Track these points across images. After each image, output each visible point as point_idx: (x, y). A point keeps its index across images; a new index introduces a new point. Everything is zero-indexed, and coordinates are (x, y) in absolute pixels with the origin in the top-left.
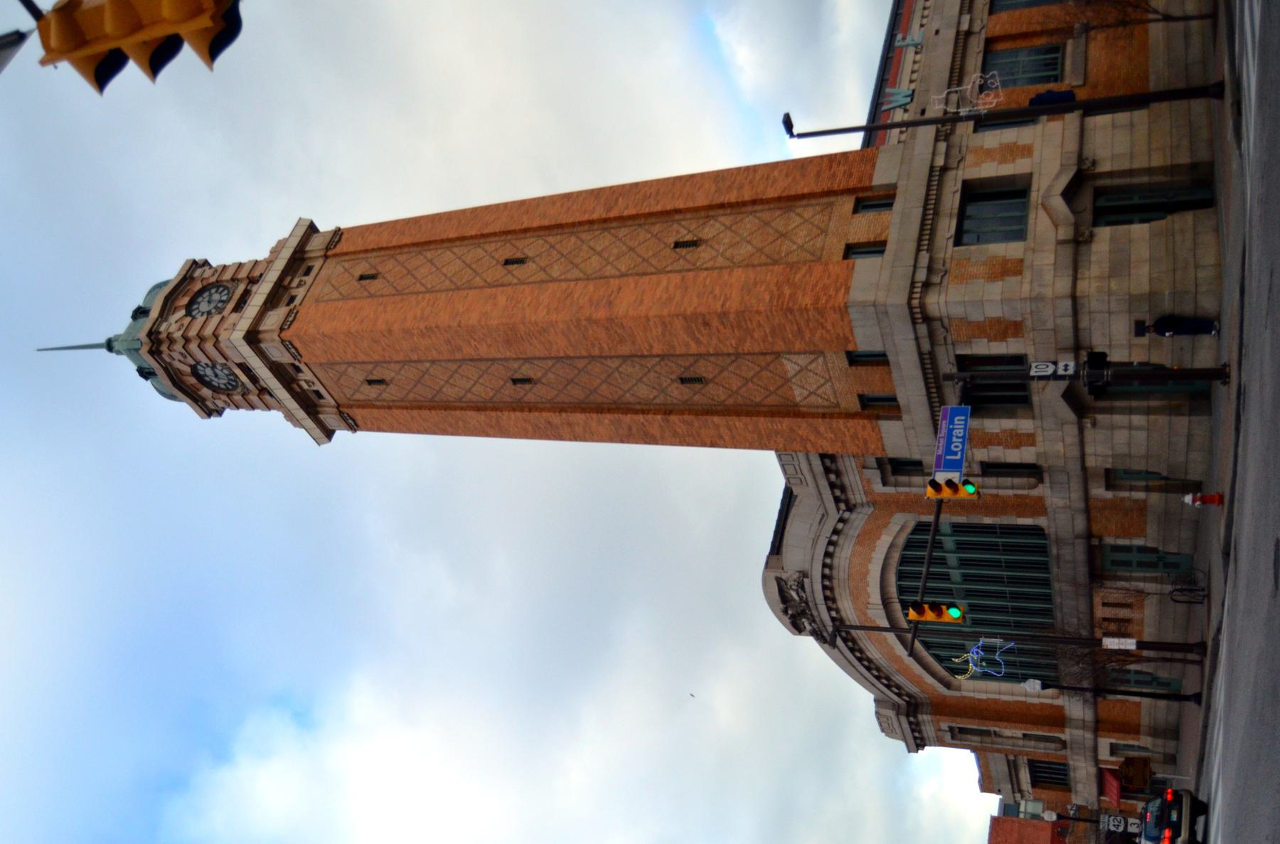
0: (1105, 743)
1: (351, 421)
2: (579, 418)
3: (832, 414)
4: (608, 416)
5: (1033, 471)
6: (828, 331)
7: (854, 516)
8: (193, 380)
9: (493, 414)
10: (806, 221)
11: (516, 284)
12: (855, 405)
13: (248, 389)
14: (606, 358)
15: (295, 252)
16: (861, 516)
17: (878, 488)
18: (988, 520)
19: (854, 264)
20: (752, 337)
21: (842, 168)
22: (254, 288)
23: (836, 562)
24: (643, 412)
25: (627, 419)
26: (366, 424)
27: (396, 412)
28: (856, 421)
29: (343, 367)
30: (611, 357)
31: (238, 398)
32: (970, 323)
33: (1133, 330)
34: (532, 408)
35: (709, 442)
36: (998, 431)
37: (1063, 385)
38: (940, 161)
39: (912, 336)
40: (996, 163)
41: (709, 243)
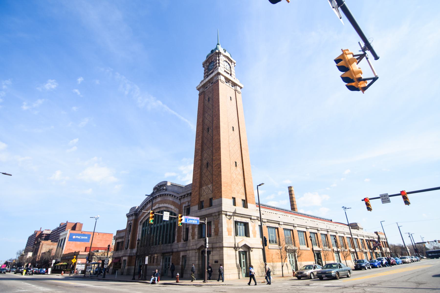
0: (126, 258)
1: (201, 94)
2: (200, 142)
3: (200, 195)
4: (201, 148)
5: (186, 240)
6: (217, 194)
7: (178, 200)
8: (210, 61)
9: (202, 124)
10: (240, 189)
11: (228, 129)
12: (201, 200)
13: (208, 72)
14: (213, 147)
15: (236, 84)
16: (178, 202)
17: (184, 205)
18: (176, 230)
19: (231, 199)
20: (216, 178)
21: (251, 197)
22: (229, 75)
23: (169, 197)
24: (201, 155)
25: (200, 152)
26: (200, 97)
27: (203, 103)
28: (198, 200)
29: (212, 93)
30: (213, 148)
31: (207, 71)
32: (218, 224)
33: (216, 260)
34: (203, 132)
35: (194, 169)
36: (195, 231)
37: (204, 245)
38: (252, 218)
39: (215, 212)
40: (252, 229)
41: (236, 169)
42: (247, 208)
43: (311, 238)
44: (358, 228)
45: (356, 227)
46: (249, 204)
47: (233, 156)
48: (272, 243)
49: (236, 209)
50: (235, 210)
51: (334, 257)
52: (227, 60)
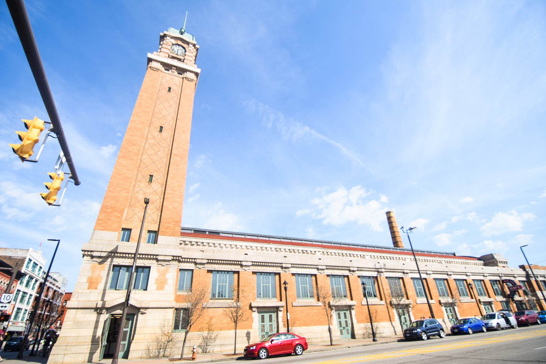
15: (186, 69)
41: (149, 186)
42: (156, 243)
43: (365, 285)
44: (496, 262)
45: (494, 259)
46: (160, 237)
47: (147, 167)
48: (220, 298)
49: (118, 246)
50: (117, 247)
51: (394, 315)
52: (180, 43)
